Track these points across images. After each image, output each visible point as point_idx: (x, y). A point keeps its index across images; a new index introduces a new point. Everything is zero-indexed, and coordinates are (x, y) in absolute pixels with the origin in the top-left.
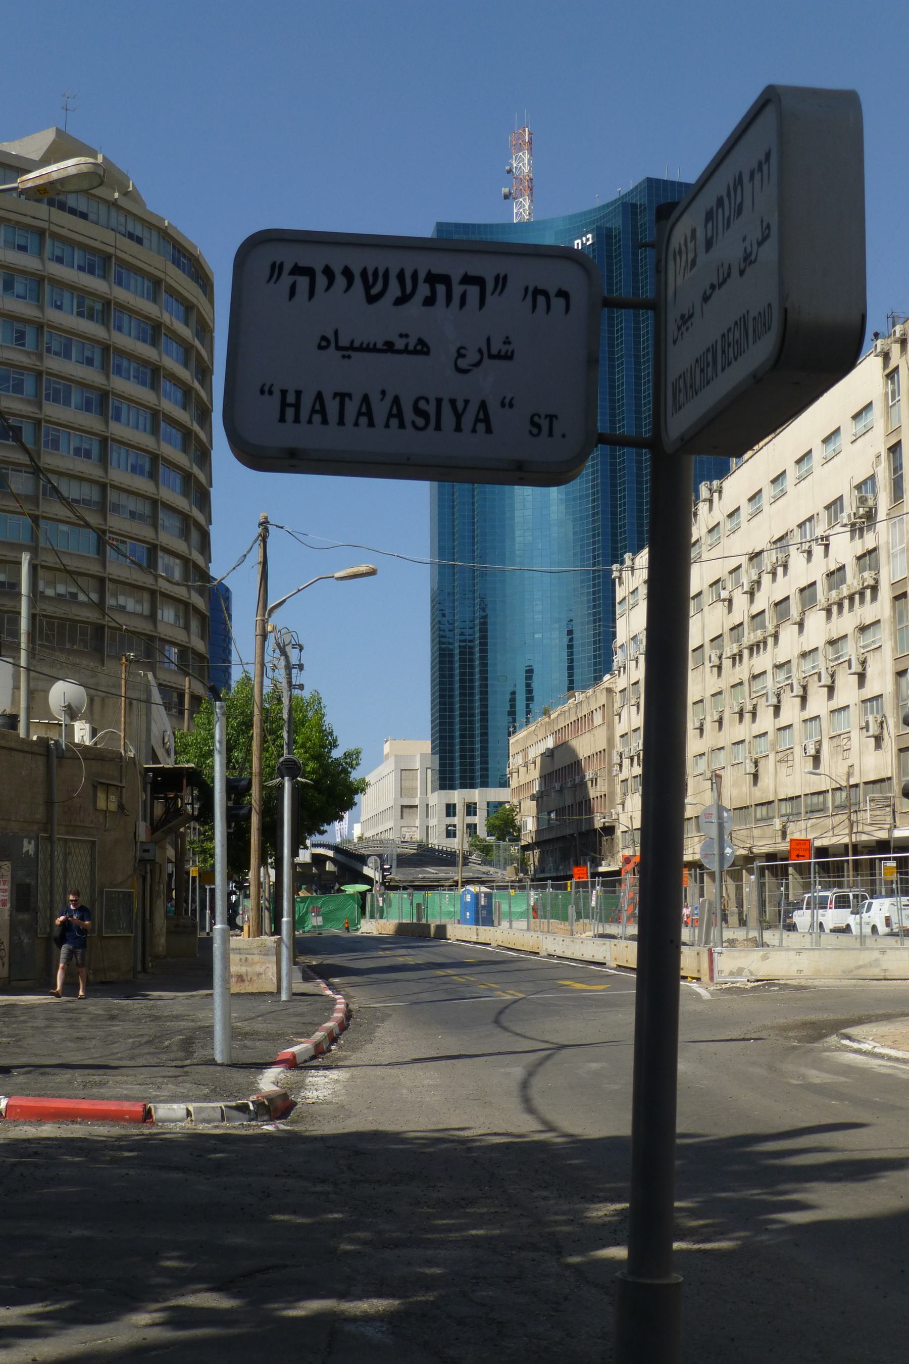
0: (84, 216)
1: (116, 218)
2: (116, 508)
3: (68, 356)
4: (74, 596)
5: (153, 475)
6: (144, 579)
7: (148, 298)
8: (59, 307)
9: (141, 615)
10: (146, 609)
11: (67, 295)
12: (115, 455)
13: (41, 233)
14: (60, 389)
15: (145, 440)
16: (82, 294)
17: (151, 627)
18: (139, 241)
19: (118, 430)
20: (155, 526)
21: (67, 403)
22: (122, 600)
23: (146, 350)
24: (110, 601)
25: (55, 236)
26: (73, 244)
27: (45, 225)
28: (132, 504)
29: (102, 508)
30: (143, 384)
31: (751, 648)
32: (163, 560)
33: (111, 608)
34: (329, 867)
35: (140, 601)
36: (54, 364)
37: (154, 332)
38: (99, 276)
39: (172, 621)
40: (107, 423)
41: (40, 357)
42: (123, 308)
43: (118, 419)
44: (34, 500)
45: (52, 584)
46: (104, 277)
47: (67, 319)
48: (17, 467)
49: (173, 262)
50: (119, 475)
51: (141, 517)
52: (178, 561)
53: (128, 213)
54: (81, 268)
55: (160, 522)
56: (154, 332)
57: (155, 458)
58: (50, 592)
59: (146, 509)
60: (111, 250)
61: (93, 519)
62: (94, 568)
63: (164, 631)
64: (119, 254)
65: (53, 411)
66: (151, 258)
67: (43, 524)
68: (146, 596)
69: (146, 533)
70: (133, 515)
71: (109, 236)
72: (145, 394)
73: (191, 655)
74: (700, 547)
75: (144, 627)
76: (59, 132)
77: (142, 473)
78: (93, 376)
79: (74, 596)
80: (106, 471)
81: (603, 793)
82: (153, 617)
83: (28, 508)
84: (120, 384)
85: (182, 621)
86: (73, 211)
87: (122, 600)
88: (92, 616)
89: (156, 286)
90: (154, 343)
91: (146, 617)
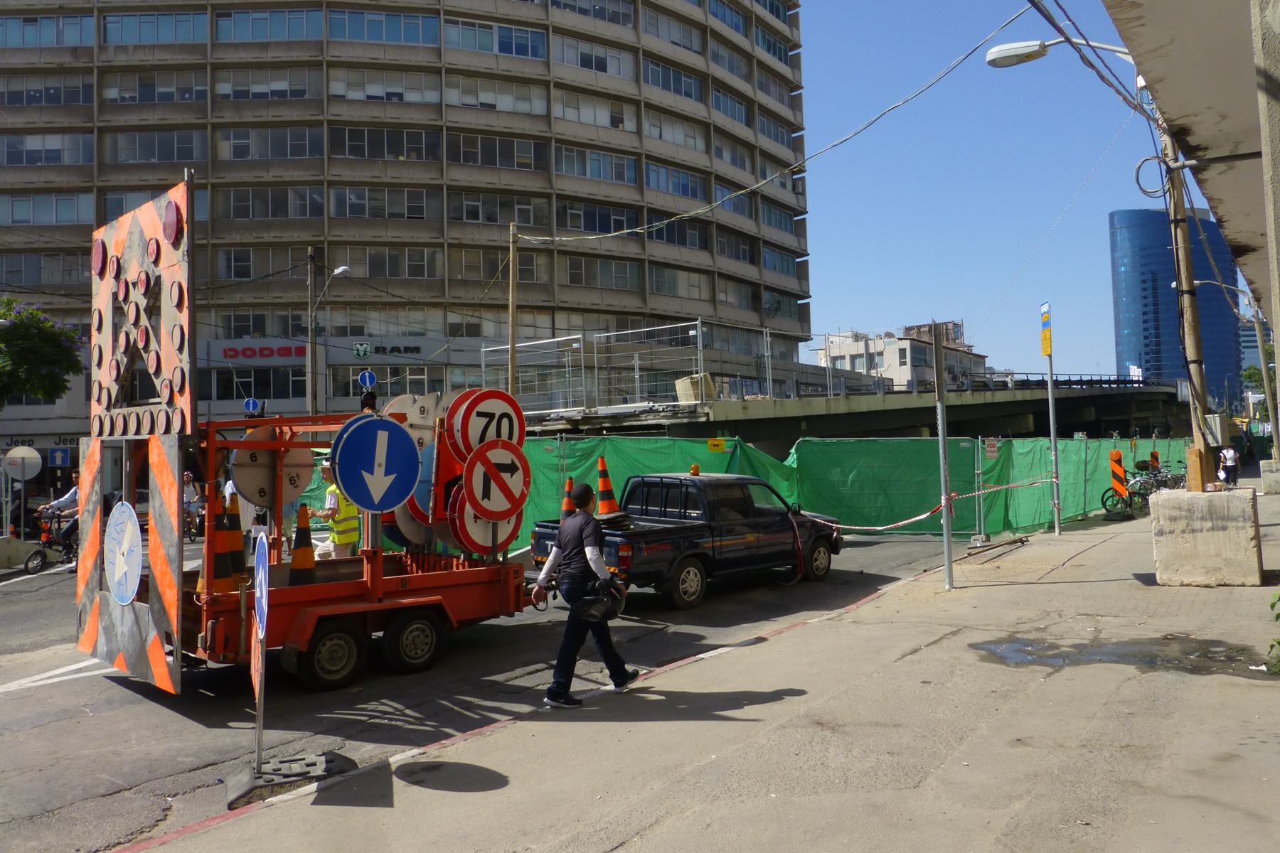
4: (400, 96)
9: (529, 116)
22: (486, 97)
45: (361, 86)
79: (400, 96)
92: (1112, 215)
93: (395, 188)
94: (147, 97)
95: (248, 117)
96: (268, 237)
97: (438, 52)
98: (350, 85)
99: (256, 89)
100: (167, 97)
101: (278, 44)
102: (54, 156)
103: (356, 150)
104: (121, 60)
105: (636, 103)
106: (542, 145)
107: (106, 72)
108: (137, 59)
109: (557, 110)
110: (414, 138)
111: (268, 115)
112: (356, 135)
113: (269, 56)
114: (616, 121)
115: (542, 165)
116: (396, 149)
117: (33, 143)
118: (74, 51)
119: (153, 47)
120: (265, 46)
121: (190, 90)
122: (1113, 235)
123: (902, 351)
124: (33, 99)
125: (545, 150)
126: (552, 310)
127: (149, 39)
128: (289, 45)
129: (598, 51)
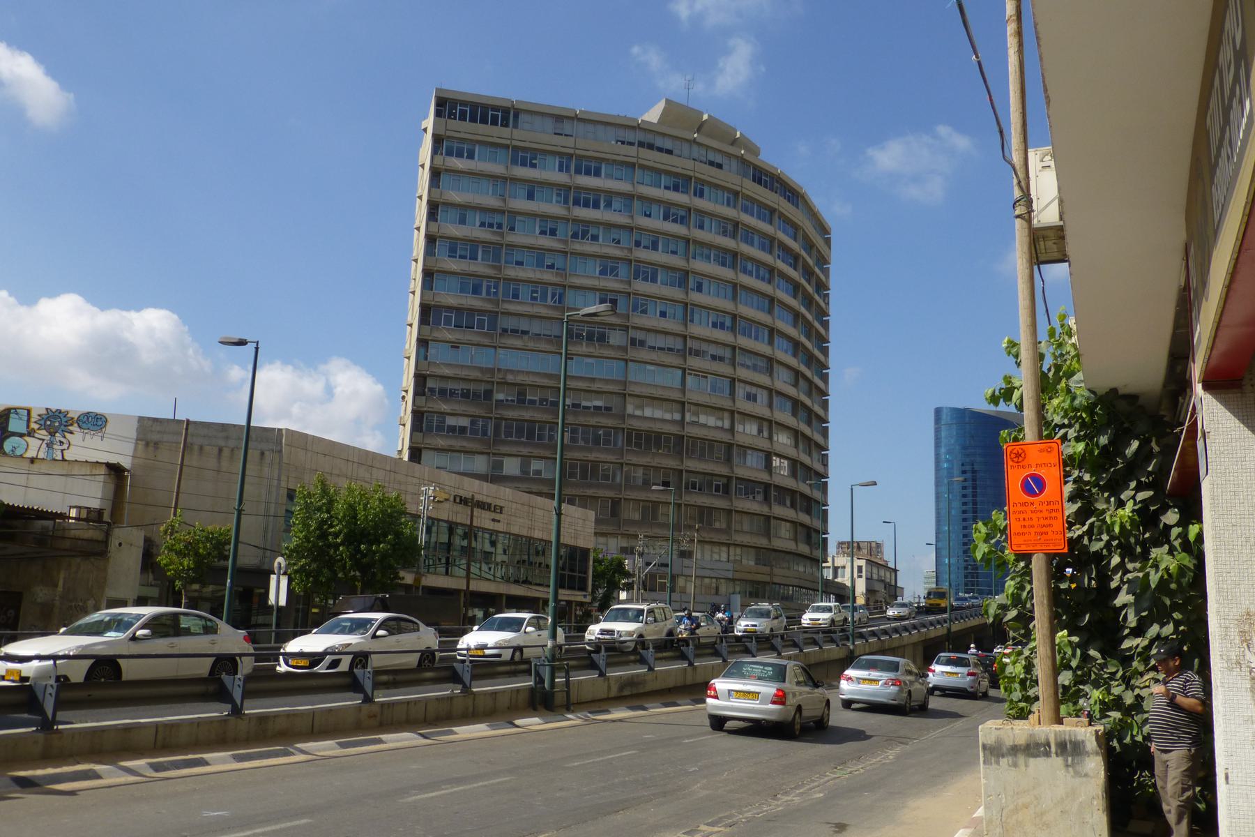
0: (669, 152)
1: (696, 152)
2: (697, 353)
3: (655, 248)
5: (733, 329)
6: (727, 404)
7: (728, 204)
8: (649, 216)
10: (727, 424)
11: (655, 208)
12: (696, 317)
13: (632, 165)
14: (650, 272)
15: (728, 305)
16: (668, 205)
17: (730, 437)
18: (720, 166)
19: (695, 297)
20: (734, 366)
21: (654, 280)
23: (728, 243)
24: (688, 417)
25: (643, 167)
26: (659, 172)
27: (634, 160)
28: (713, 350)
29: (683, 353)
30: (724, 264)
32: (741, 390)
33: (693, 423)
35: (722, 419)
36: (642, 254)
37: (733, 228)
39: (755, 431)
41: (630, 250)
42: (701, 213)
43: (699, 288)
44: (625, 349)
46: (686, 192)
47: (656, 223)
48: (612, 326)
49: (754, 180)
50: (696, 329)
51: (721, 359)
52: (760, 390)
53: (708, 147)
54: (666, 188)
56: (733, 228)
58: (638, 413)
59: (727, 353)
60: (691, 173)
61: (677, 361)
62: (676, 395)
63: (740, 439)
64: (578, 152)
65: (641, 286)
66: (730, 177)
67: (630, 364)
68: (726, 415)
69: (725, 369)
70: (714, 357)
71: (689, 164)
72: (727, 273)
75: (726, 437)
76: (668, 101)
77: (722, 326)
78: (677, 261)
80: (686, 326)
82: (732, 430)
83: (619, 354)
84: (699, 265)
85: (766, 434)
86: (660, 150)
87: (703, 419)
88: (674, 429)
89: (734, 196)
90: (734, 237)
91: (726, 430)
92: (938, 412)
93: (657, 468)
94: (521, 400)
95: (581, 420)
96: (590, 492)
97: (683, 391)
98: (637, 407)
99: (584, 403)
100: (532, 402)
101: (600, 380)
102: (463, 430)
103: (638, 445)
104: (510, 378)
105: (770, 422)
106: (730, 446)
107: (503, 383)
108: (520, 379)
109: (739, 428)
110: (668, 440)
111: (593, 421)
112: (639, 436)
113: (595, 386)
114: (760, 431)
115: (728, 460)
116: (658, 446)
117: (451, 421)
118: (481, 369)
119: (528, 373)
120: (593, 380)
121: (546, 400)
122: (937, 431)
123: (860, 568)
124: (453, 393)
125: (730, 451)
126: (728, 545)
127: (523, 366)
128: (607, 381)
129: (753, 390)
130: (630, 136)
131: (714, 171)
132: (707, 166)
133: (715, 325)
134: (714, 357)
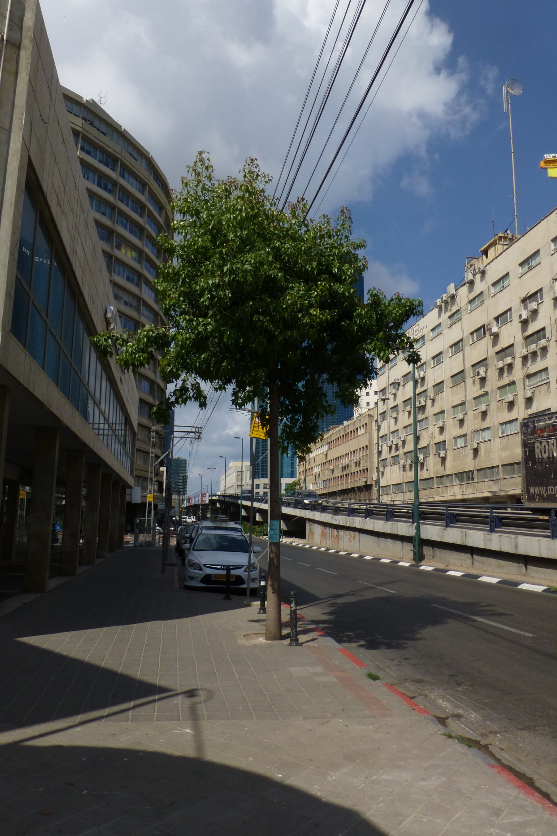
12: (116, 269)
31: (525, 359)
34: (218, 505)
37: (141, 208)
38: (111, 169)
40: (112, 249)
46: (114, 170)
51: (131, 306)
54: (100, 161)
55: (141, 311)
57: (140, 275)
60: (119, 156)
73: (156, 388)
74: (461, 313)
77: (132, 282)
81: (365, 468)
85: (152, 369)
86: (98, 130)
89: (143, 185)
130: (76, 110)
131: (133, 161)
132: (129, 155)
133: (128, 279)
134: (126, 303)
